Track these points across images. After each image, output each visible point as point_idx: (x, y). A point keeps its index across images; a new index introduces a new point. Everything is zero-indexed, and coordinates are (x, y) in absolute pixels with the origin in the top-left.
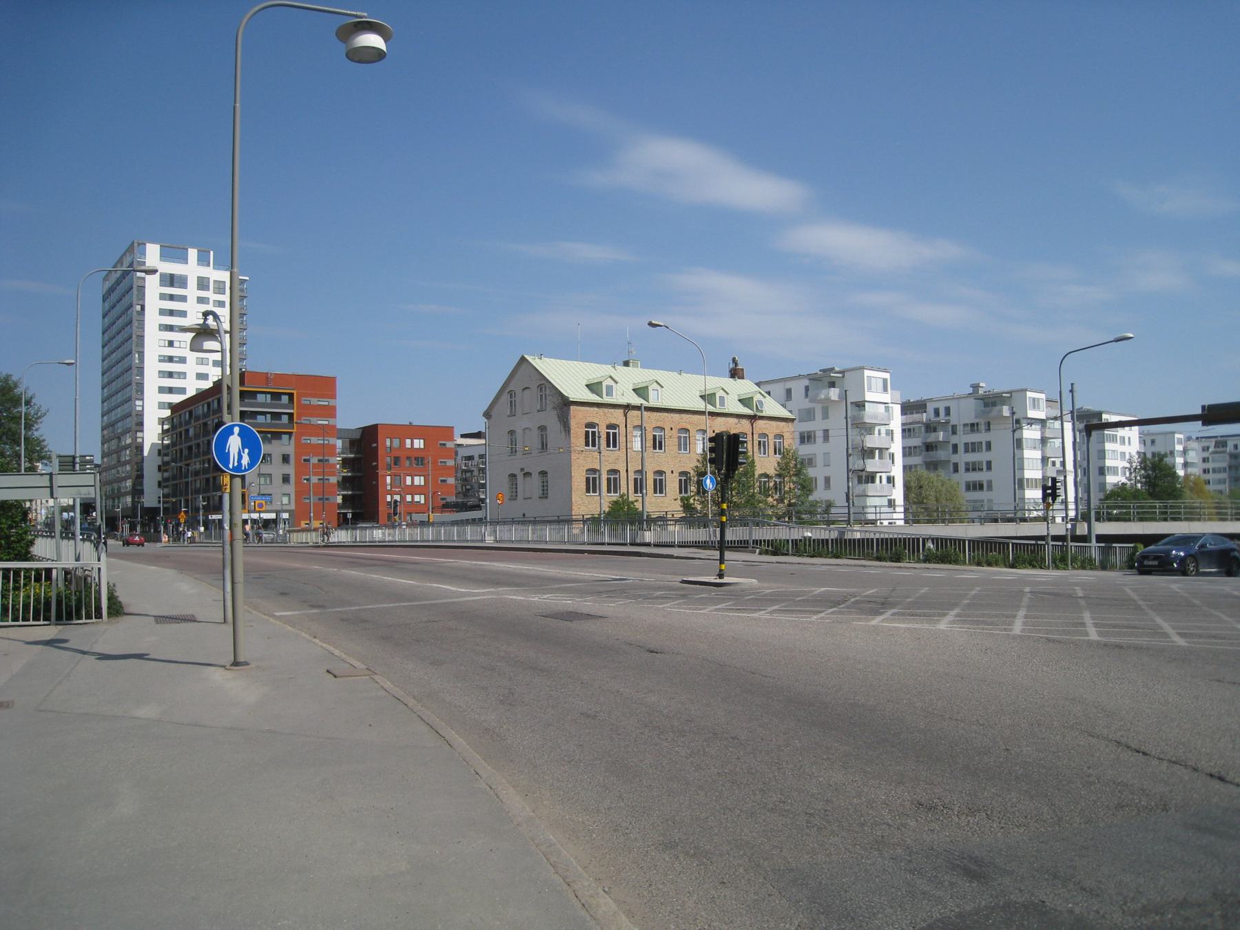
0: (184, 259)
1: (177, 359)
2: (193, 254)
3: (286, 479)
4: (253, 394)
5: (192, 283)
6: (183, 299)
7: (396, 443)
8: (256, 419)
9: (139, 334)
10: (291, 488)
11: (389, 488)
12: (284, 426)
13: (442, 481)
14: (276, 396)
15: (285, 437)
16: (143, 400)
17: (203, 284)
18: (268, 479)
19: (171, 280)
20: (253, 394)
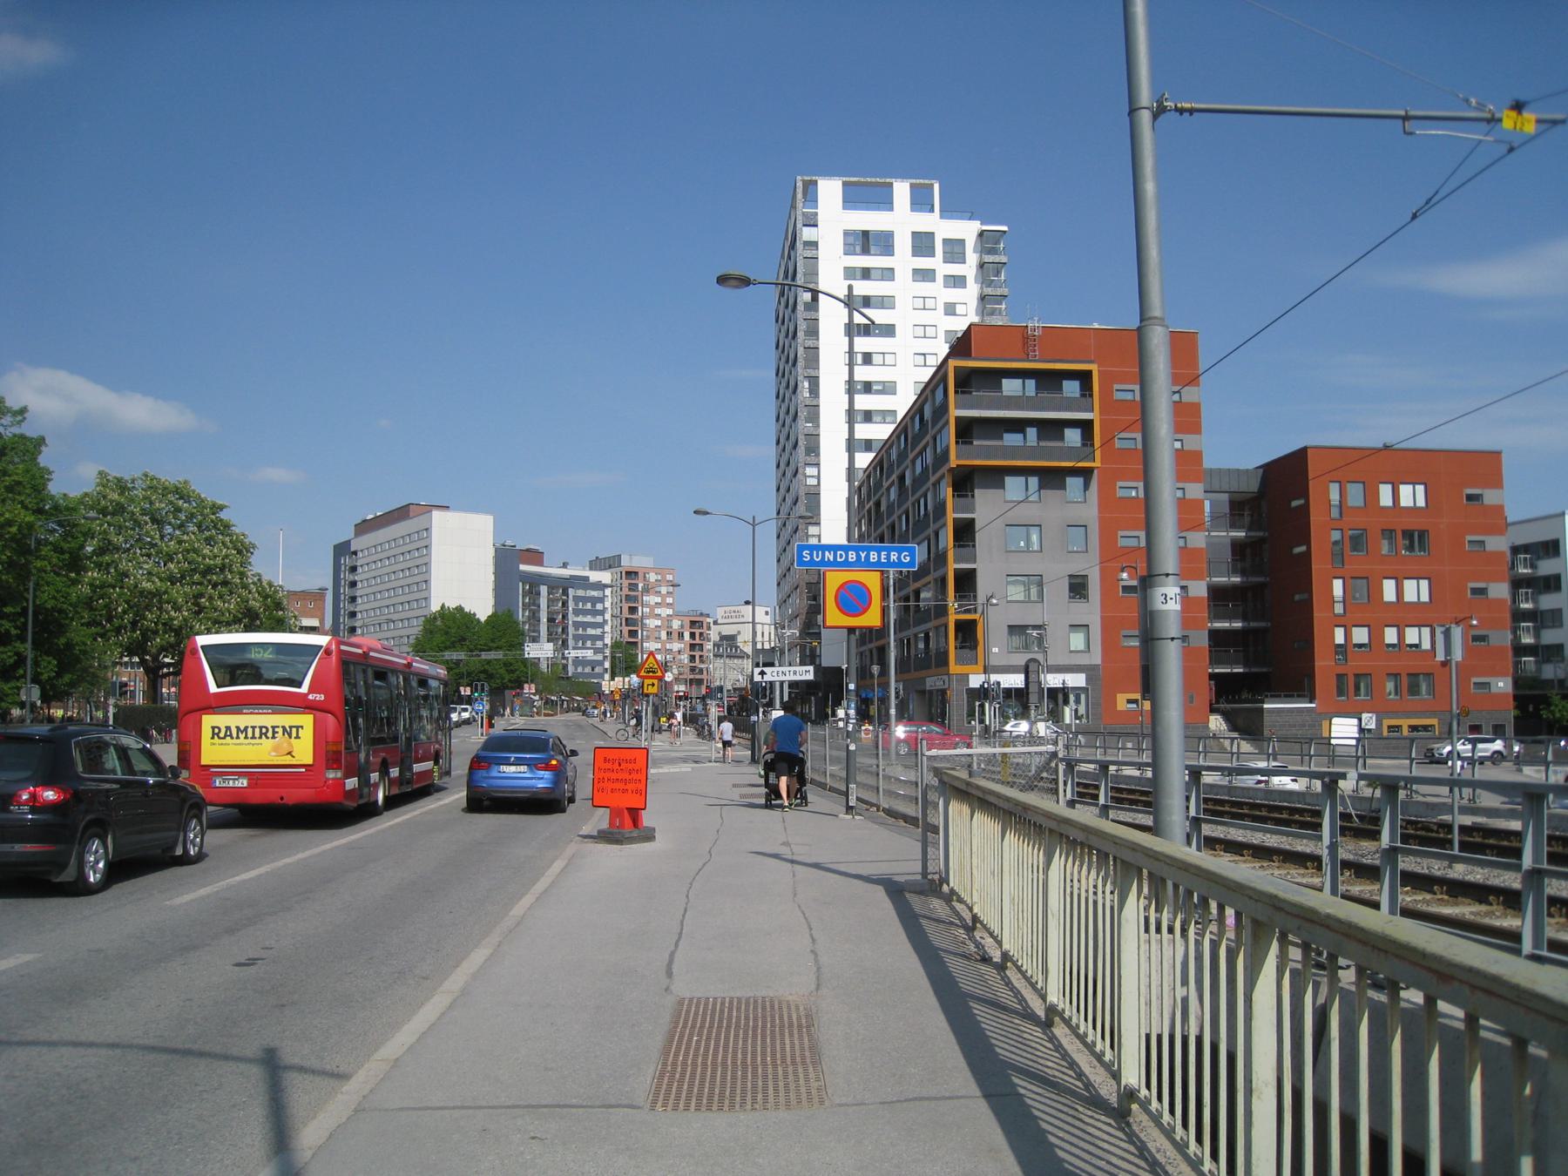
0: (885, 202)
1: (880, 388)
2: (902, 190)
3: (1078, 588)
4: (993, 377)
5: (903, 244)
6: (888, 274)
7: (1355, 495)
8: (1001, 438)
9: (810, 343)
10: (1091, 611)
11: (1339, 609)
12: (1070, 453)
13: (1475, 591)
14: (1049, 380)
15: (1074, 483)
16: (818, 465)
17: (922, 243)
18: (1034, 590)
19: (864, 241)
20: (993, 377)
